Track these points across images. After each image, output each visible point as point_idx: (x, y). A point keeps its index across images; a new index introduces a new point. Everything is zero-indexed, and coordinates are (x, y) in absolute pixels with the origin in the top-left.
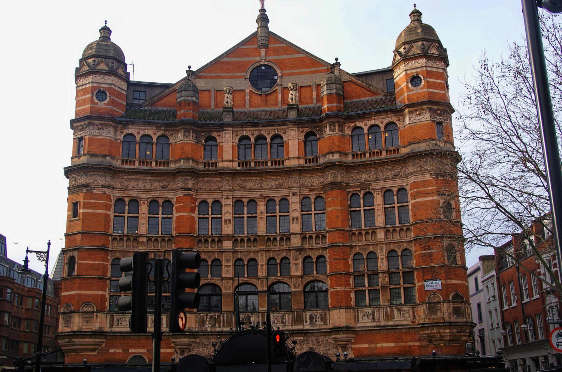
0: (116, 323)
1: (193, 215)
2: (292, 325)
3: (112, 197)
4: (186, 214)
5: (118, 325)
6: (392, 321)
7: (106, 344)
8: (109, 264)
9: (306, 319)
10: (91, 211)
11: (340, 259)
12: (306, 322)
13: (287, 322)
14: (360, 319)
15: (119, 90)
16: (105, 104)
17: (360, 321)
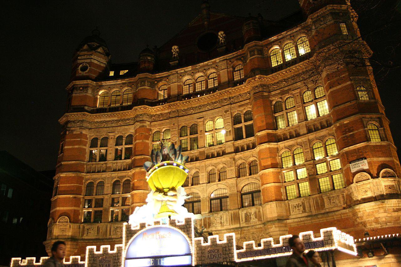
0: (86, 232)
1: (147, 141)
2: (230, 225)
3: (88, 136)
4: (141, 141)
5: (88, 234)
6: (323, 209)
7: (78, 250)
8: (83, 186)
9: (242, 217)
10: (71, 147)
11: (267, 158)
12: (242, 221)
13: (225, 222)
14: (291, 212)
15: (98, 63)
16: (86, 73)
17: (292, 214)
